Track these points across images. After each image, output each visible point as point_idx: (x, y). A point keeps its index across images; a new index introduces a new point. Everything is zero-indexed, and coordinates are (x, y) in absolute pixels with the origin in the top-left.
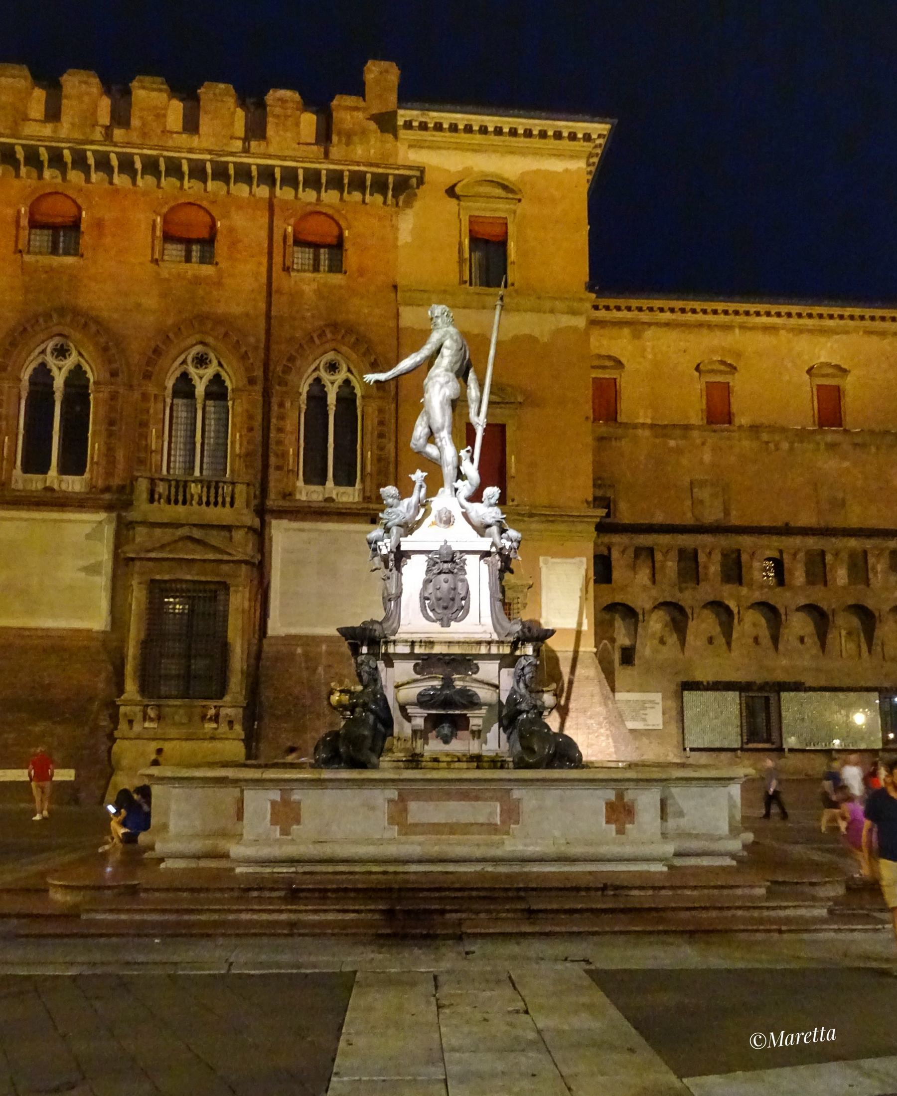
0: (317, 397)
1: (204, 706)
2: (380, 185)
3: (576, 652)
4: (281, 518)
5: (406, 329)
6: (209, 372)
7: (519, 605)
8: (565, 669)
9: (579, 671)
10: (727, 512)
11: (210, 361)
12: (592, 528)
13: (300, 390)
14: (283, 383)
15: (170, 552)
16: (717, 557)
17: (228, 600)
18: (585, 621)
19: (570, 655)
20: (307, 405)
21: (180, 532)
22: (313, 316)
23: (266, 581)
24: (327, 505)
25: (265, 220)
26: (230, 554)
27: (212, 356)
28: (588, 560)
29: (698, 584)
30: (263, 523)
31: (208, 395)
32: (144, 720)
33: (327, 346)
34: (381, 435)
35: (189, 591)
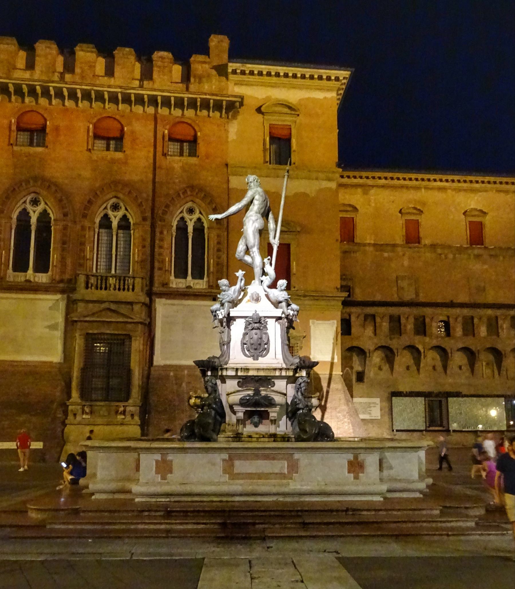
0: (182, 228)
1: (117, 406)
2: (218, 106)
3: (331, 375)
4: (161, 298)
5: (233, 189)
6: (120, 214)
7: (298, 348)
8: (324, 384)
9: (332, 385)
10: (417, 294)
11: (121, 208)
12: (340, 304)
13: (172, 224)
14: (162, 220)
15: (98, 317)
16: (412, 320)
17: (131, 345)
18: (336, 357)
19: (327, 376)
20: (176, 233)
21: (103, 306)
22: (180, 182)
23: (152, 334)
24: (188, 290)
25: (152, 127)
26: (132, 318)
27: (122, 204)
28: (337, 322)
29: (401, 335)
30: (151, 301)
31: (120, 227)
32: (83, 414)
33: (188, 199)
34: (219, 250)
35: (108, 339)
